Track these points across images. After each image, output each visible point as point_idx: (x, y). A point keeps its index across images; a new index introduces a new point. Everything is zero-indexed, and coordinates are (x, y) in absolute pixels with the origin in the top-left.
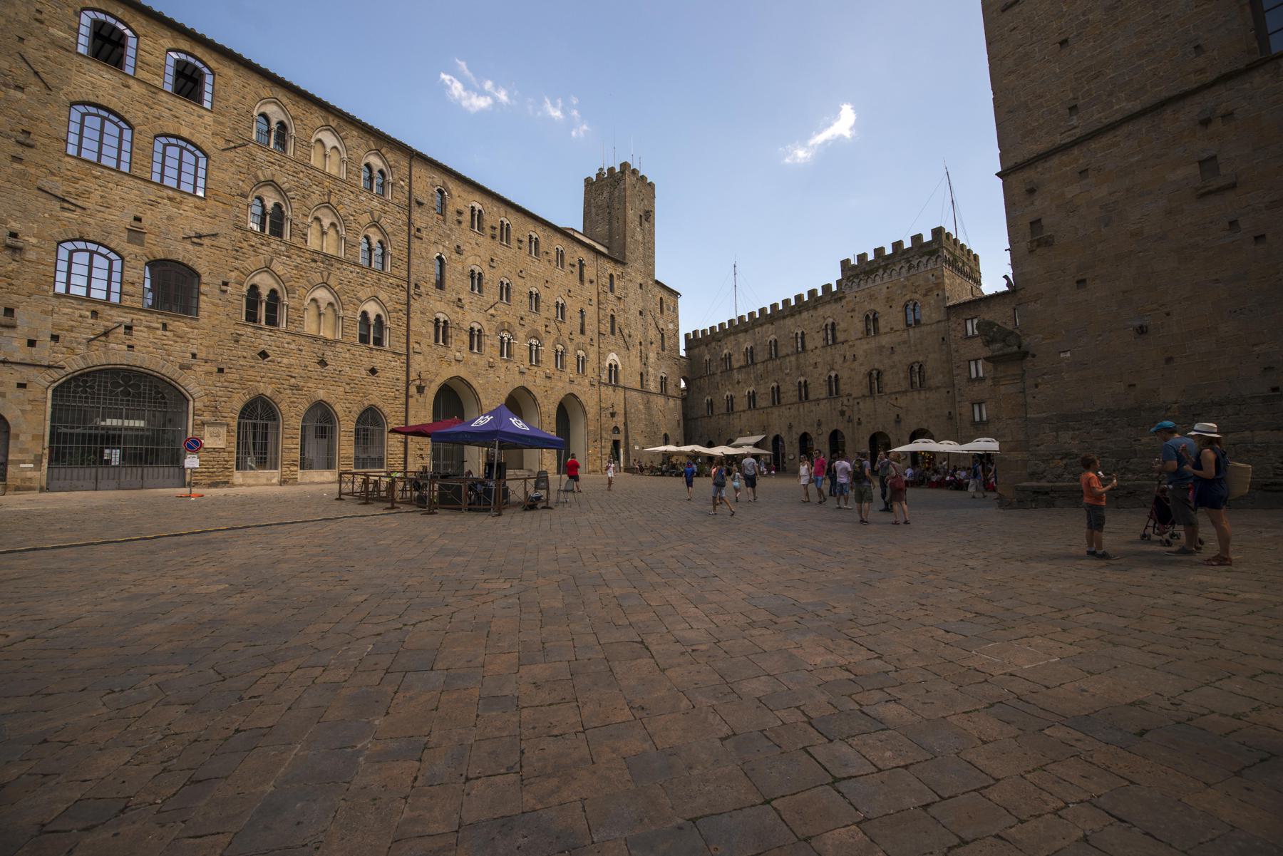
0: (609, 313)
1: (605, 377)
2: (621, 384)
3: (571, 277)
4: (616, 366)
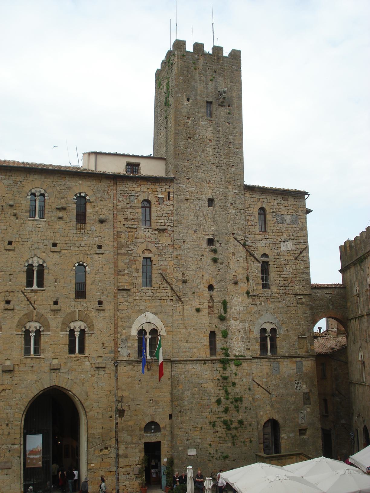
1: (128, 351)
3: (58, 225)
4: (154, 332)
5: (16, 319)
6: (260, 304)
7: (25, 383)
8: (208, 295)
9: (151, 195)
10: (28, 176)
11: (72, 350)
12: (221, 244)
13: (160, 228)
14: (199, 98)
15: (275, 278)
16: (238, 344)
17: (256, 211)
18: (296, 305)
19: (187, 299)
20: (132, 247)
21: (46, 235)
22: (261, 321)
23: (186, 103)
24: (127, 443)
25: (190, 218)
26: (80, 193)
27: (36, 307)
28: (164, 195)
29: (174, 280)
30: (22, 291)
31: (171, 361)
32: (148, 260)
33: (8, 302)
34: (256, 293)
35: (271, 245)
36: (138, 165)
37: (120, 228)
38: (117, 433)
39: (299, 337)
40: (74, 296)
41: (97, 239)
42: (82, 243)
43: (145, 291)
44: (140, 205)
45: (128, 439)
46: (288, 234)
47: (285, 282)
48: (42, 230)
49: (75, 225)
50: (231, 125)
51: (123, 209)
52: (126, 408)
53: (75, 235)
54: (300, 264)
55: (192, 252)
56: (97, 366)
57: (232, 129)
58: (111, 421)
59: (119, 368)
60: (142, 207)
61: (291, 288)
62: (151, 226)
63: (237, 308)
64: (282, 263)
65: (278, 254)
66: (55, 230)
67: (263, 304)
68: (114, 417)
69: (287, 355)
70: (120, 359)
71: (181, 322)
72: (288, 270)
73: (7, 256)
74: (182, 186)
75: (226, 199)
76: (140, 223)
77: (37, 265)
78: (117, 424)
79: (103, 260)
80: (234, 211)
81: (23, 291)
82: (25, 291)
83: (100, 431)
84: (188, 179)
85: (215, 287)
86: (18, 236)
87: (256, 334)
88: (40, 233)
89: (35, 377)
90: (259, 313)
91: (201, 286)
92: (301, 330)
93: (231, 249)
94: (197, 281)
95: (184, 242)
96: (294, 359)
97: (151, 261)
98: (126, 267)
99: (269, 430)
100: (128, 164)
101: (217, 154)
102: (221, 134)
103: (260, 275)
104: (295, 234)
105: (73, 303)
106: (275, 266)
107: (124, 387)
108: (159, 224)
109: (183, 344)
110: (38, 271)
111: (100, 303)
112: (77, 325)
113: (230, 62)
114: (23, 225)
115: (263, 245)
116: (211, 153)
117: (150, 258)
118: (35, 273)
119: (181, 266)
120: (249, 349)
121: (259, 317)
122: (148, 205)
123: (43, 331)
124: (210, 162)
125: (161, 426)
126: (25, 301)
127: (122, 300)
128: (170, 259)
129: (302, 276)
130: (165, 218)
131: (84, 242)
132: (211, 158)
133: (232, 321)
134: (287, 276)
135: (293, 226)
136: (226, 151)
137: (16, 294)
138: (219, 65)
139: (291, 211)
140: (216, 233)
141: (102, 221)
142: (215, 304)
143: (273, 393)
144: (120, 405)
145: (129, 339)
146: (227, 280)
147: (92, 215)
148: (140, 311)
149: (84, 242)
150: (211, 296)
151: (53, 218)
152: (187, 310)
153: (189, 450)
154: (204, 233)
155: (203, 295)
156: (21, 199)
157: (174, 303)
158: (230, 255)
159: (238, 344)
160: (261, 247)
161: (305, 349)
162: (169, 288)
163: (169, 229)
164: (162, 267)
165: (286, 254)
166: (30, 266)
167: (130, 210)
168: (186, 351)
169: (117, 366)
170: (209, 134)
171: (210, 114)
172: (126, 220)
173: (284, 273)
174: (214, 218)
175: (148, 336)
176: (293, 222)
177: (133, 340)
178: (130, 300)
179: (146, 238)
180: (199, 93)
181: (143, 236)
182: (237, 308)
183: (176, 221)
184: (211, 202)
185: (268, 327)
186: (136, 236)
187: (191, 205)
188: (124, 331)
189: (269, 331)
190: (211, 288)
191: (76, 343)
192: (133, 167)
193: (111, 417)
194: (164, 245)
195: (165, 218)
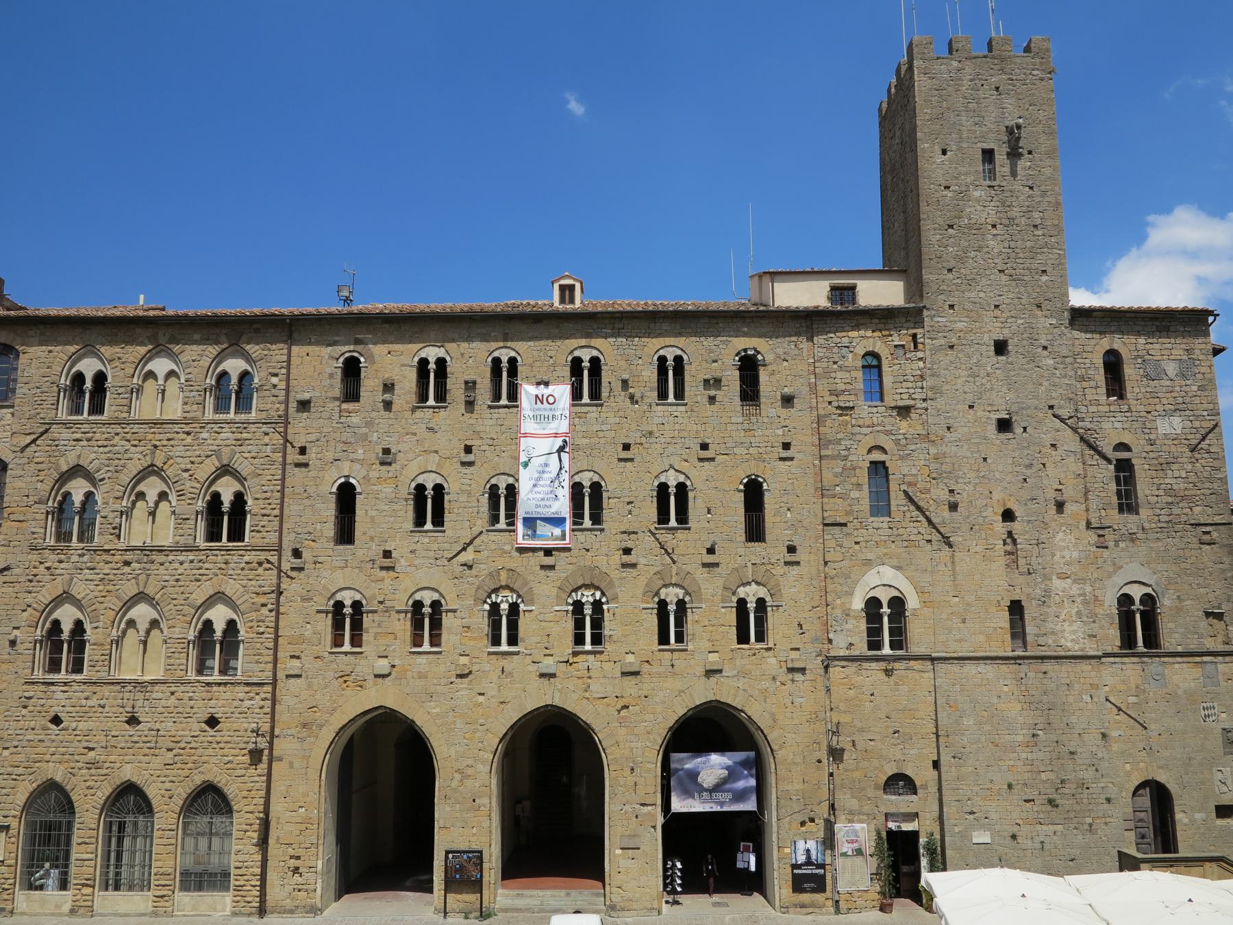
0: (861, 459)
2: (915, 648)
4: (898, 604)
5: (642, 581)
7: (661, 694)
8: (1004, 531)
10: (652, 325)
11: (743, 638)
12: (1025, 429)
13: (901, 403)
15: (1148, 492)
20: (848, 443)
24: (851, 813)
25: (959, 381)
26: (745, 350)
30: (650, 531)
31: (933, 660)
32: (880, 467)
33: (627, 551)
34: (1106, 523)
35: (1136, 425)
36: (853, 288)
37: (824, 409)
38: (832, 792)
40: (743, 538)
41: (780, 432)
42: (753, 440)
44: (860, 363)
45: (854, 804)
46: (1171, 400)
47: (1170, 500)
48: (680, 420)
49: (739, 408)
50: (1036, 191)
51: (827, 373)
52: (848, 747)
53: (740, 427)
54: (1204, 460)
56: (790, 666)
58: (819, 769)
59: (831, 670)
60: (863, 367)
61: (1185, 511)
62: (882, 400)
63: (1067, 553)
64: (1162, 461)
65: (1152, 443)
66: (705, 420)
67: (1122, 545)
68: (825, 761)
69: (1180, 649)
70: (832, 653)
71: (951, 583)
72: (1177, 474)
75: (1033, 340)
76: (862, 397)
78: (831, 775)
79: (793, 470)
80: (1052, 362)
83: (799, 786)
84: (952, 307)
85: (1017, 514)
86: (639, 434)
87: (1110, 605)
88: (677, 427)
89: (678, 684)
90: (1114, 564)
91: (988, 512)
92: (1211, 597)
93: (1047, 439)
94: (980, 503)
95: (949, 428)
96: (1198, 659)
97: (886, 469)
98: (837, 481)
99: (1145, 801)
100: (834, 289)
103: (1113, 487)
104: (1188, 400)
105: (742, 551)
106: (1147, 467)
107: (842, 707)
108: (898, 397)
110: (676, 495)
111: (792, 549)
112: (751, 593)
113: (1027, 64)
114: (648, 414)
116: (996, 250)
117: (884, 463)
118: (672, 499)
120: (1095, 636)
121: (1115, 572)
122: (875, 363)
123: (692, 601)
125: (918, 783)
126: (658, 550)
127: (831, 543)
128: (922, 462)
129: (1207, 485)
130: (910, 385)
131: (757, 439)
133: (1057, 583)
134: (1175, 487)
136: (1028, 244)
137: (641, 535)
139: (1178, 352)
140: (1014, 408)
141: (788, 400)
143: (1153, 727)
144: (835, 738)
145: (848, 615)
147: (770, 389)
148: (868, 564)
149: (757, 439)
150: (1010, 534)
153: (975, 834)
157: (935, 545)
160: (1111, 431)
161: (1220, 638)
162: (921, 518)
164: (907, 479)
165: (1170, 442)
166: (663, 488)
167: (839, 374)
168: (960, 641)
169: (826, 668)
170: (989, 214)
172: (832, 393)
173: (1167, 481)
175: (885, 610)
177: (855, 618)
178: (848, 543)
182: (1067, 553)
183: (932, 388)
184: (1001, 348)
185: (1137, 592)
186: (854, 422)
188: (838, 601)
189: (1137, 601)
190: (1008, 516)
191: (750, 623)
192: (843, 293)
193: (819, 761)
195: (910, 385)
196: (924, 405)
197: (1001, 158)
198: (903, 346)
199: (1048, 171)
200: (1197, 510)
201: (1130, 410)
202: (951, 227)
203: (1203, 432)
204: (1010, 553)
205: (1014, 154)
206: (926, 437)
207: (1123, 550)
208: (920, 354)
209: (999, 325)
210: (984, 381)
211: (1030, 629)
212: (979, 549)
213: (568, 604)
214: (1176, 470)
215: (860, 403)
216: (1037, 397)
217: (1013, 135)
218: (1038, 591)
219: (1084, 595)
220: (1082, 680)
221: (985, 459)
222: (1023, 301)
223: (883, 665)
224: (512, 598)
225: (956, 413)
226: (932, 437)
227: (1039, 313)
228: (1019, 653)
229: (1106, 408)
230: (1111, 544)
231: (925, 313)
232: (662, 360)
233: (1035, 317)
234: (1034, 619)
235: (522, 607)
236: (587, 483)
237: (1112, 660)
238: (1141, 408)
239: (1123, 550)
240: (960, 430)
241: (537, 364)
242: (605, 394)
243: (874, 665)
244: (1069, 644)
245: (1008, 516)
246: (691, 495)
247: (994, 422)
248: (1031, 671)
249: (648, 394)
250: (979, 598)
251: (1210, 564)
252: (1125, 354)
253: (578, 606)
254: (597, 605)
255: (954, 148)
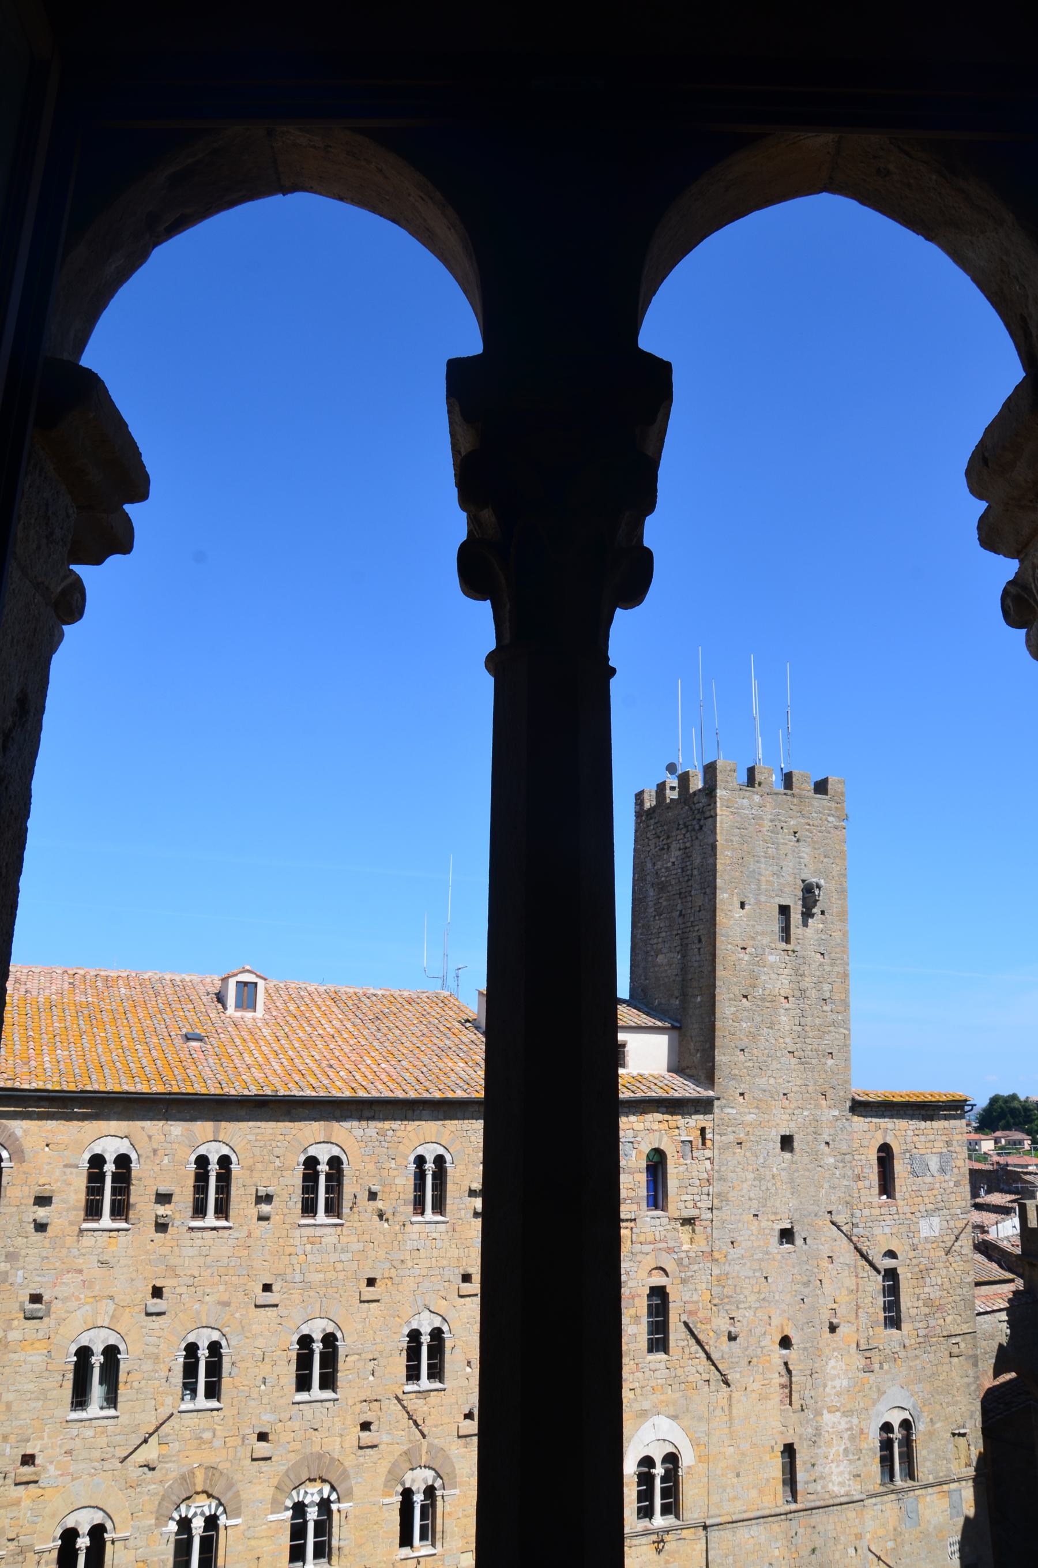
4: (672, 1459)
6: (881, 1368)
9: (665, 1139)
12: (805, 1239)
13: (686, 1214)
14: (763, 898)
15: (909, 1304)
16: (838, 1466)
17: (873, 1156)
18: (947, 1359)
19: (738, 1376)
21: (448, 1255)
22: (881, 1407)
23: (738, 913)
25: (745, 1185)
27: (426, 1433)
28: (694, 1136)
29: (712, 1334)
30: (397, 1398)
31: (705, 1527)
35: (903, 1229)
39: (954, 1435)
43: (653, 1366)
47: (927, 1310)
50: (827, 960)
55: (748, 1264)
57: (828, 968)
63: (837, 1383)
64: (922, 1267)
67: (886, 1366)
71: (727, 1431)
73: (364, 1315)
74: (730, 1110)
76: (644, 1204)
77: (429, 1330)
80: (832, 1160)
81: (401, 1396)
82: (404, 1397)
84: (742, 1094)
86: (388, 1265)
88: (435, 1253)
90: (879, 1389)
94: (759, 1331)
95: (732, 1243)
96: (945, 1487)
101: (799, 1028)
102: (807, 983)
106: (909, 1275)
108: (682, 1205)
109: (729, 1482)
114: (400, 1237)
115: (887, 1230)
116: (787, 1028)
119: (726, 1300)
120: (859, 1476)
124: (785, 1048)
129: (959, 1291)
132: (788, 1040)
133: (828, 1418)
135: (942, 1179)
136: (817, 1021)
137: (385, 1403)
138: (804, 817)
139: (940, 1146)
140: (796, 1216)
142: (793, 1379)
146: (817, 1322)
151: (463, 1212)
152: (739, 1401)
154: (773, 1218)
155: (769, 1362)
156: (395, 1173)
158: (825, 1263)
159: (838, 1466)
160: (881, 1238)
162: (702, 1355)
163: (703, 1217)
164: (689, 1307)
171: (786, 934)
173: (926, 1290)
174: (792, 1181)
175: (659, 1471)
176: (942, 1170)
179: (655, 1242)
180: (763, 887)
181: (650, 1238)
183: (719, 1195)
185: (896, 1421)
187: (748, 1154)
190: (785, 1342)
194: (694, 1255)
196: (709, 1215)
197: (796, 917)
198: (690, 1142)
199: (837, 935)
200: (949, 1319)
201: (898, 1213)
202: (746, 997)
203: (956, 1232)
204: (783, 1386)
205: (807, 914)
206: (710, 1255)
207: (887, 1372)
208: (708, 1153)
209: (787, 1117)
210: (770, 1185)
211: (801, 1476)
212: (756, 1386)
213: (287, 1509)
214: (934, 1278)
215: (642, 1213)
216: (816, 1202)
217: (809, 893)
218: (810, 1430)
219: (850, 1429)
220: (847, 1529)
221: (766, 1278)
222: (811, 1089)
223: (654, 1538)
224: (208, 1506)
225: (740, 1225)
226: (716, 1255)
227: (824, 1102)
228: (793, 1507)
229: (876, 1211)
230: (876, 1366)
231: (716, 1103)
232: (420, 1160)
233: (817, 1106)
234: (804, 1463)
235: (222, 1521)
236: (317, 1336)
237: (873, 1500)
238: (907, 1209)
239: (887, 1372)
240: (744, 1244)
241: (259, 1166)
242: (346, 1204)
243: (644, 1540)
244: (836, 1489)
245: (785, 1342)
246: (448, 1344)
247: (777, 1234)
248: (800, 1525)
249: (402, 1209)
250: (754, 1445)
251: (957, 1379)
252: (896, 1150)
253: (299, 1509)
254: (324, 1505)
255: (752, 901)
